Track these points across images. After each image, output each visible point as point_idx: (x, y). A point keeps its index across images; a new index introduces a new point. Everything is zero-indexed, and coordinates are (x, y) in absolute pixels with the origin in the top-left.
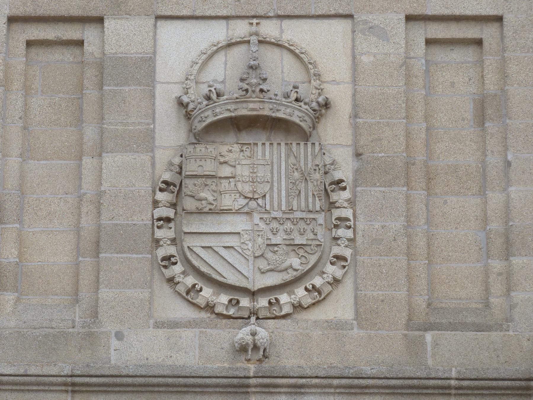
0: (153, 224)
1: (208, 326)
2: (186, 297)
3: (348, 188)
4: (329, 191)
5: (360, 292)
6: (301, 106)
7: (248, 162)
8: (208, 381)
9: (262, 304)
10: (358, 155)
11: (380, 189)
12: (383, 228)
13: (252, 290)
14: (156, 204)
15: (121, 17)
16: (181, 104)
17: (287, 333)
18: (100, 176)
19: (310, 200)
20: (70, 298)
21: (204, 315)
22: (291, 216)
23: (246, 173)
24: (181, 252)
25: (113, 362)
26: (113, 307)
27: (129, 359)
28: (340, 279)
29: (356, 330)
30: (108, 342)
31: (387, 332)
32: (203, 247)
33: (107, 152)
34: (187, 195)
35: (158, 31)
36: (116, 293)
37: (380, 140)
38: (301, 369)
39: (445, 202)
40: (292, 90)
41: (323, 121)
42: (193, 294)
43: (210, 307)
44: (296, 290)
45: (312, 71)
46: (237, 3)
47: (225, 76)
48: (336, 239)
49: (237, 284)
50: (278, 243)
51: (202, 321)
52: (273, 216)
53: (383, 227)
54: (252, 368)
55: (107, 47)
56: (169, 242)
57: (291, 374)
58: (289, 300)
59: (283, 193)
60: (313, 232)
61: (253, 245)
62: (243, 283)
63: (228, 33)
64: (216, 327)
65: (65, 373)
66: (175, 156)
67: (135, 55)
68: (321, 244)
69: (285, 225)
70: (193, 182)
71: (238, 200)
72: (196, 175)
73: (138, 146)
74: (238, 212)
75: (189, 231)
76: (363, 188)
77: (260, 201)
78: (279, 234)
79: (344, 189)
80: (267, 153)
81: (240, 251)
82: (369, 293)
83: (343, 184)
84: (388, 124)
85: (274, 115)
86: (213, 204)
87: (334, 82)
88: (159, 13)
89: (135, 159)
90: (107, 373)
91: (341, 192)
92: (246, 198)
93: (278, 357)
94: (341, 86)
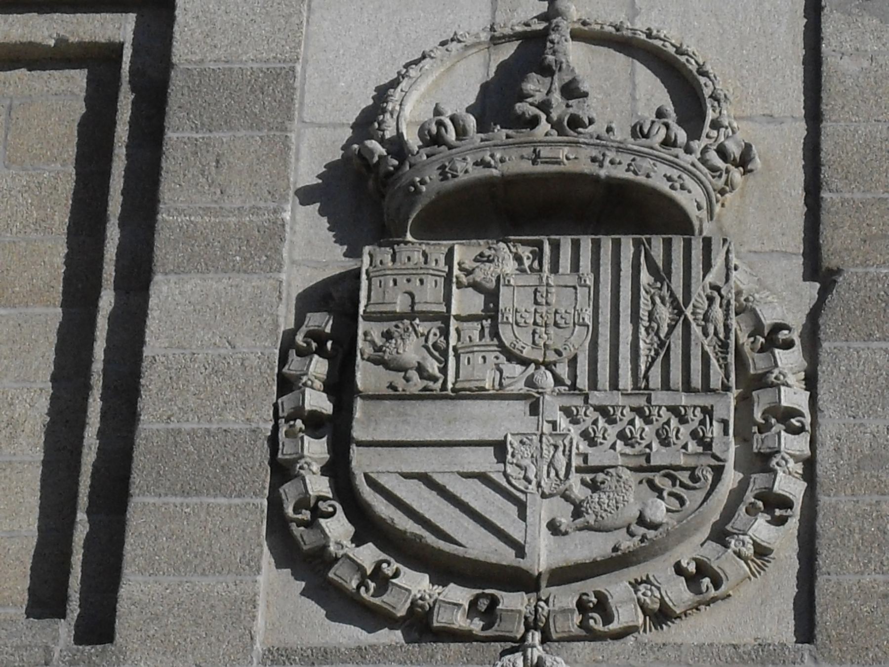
6: (677, 157)
9: (560, 605)
19: (696, 365)
26: (156, 617)
62: (506, 556)
67: (250, 64)
68: (721, 463)
83: (783, 335)
85: (603, 173)
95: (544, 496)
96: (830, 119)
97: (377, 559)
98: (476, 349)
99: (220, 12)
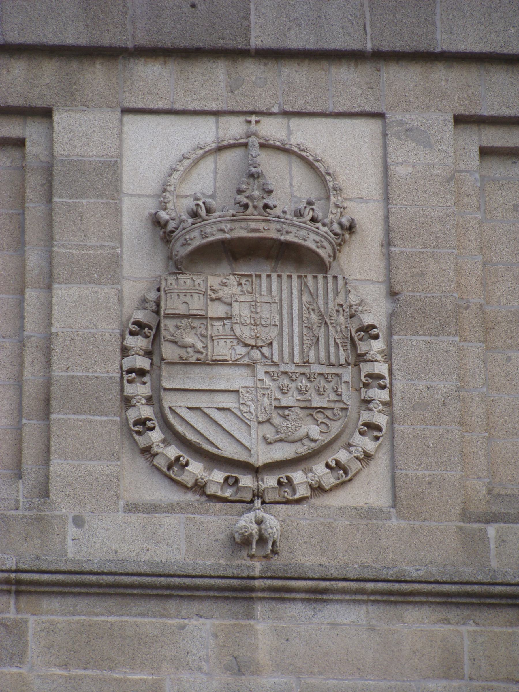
0: (122, 377)
1: (197, 512)
2: (168, 473)
3: (381, 335)
4: (356, 339)
5: (399, 471)
6: (318, 228)
7: (248, 298)
8: (199, 582)
9: (269, 484)
10: (393, 294)
11: (424, 338)
12: (428, 390)
13: (257, 466)
14: (125, 351)
15: (74, 108)
16: (157, 222)
17: (303, 523)
18: (50, 315)
19: (332, 349)
20: (10, 472)
21: (191, 497)
22: (306, 370)
23: (246, 313)
24: (159, 415)
25: (70, 555)
26: (69, 484)
27: (92, 551)
28: (373, 453)
29: (394, 520)
30: (62, 530)
31: (436, 524)
32: (189, 408)
33: (59, 283)
34: (167, 340)
35: (125, 129)
36: (73, 466)
37: (423, 275)
38: (323, 569)
39: (509, 359)
40: (306, 207)
41: (345, 249)
42: (176, 469)
43: (199, 486)
44: (313, 467)
45: (331, 184)
46: (229, 94)
47: (215, 188)
48: (367, 402)
49: (236, 457)
50: (290, 405)
51: (189, 504)
52: (282, 369)
53: (428, 388)
54: (258, 567)
55: (57, 147)
56: (144, 401)
57: (310, 575)
58: (306, 480)
59: (296, 340)
60: (336, 391)
61: (256, 408)
63: (217, 133)
64: (207, 512)
65: (8, 567)
66: (150, 289)
67: (94, 158)
68: (346, 407)
69: (298, 381)
70: (175, 324)
71: (236, 348)
72: (179, 314)
73: (100, 277)
74: (235, 364)
75: (171, 387)
76: (401, 337)
77: (266, 350)
78: (290, 393)
79: (376, 337)
80: (274, 288)
81: (239, 414)
82: (411, 473)
83: (375, 331)
84: (433, 255)
85: (282, 238)
86: (202, 353)
87: (361, 199)
88: (127, 105)
89: (96, 292)
90: (64, 568)
91: (372, 342)
92: (246, 345)
93: (291, 553)
94: (370, 205)
95: (260, 423)
96: (393, 203)
97: (177, 455)
98: (221, 337)
99: (76, 125)
